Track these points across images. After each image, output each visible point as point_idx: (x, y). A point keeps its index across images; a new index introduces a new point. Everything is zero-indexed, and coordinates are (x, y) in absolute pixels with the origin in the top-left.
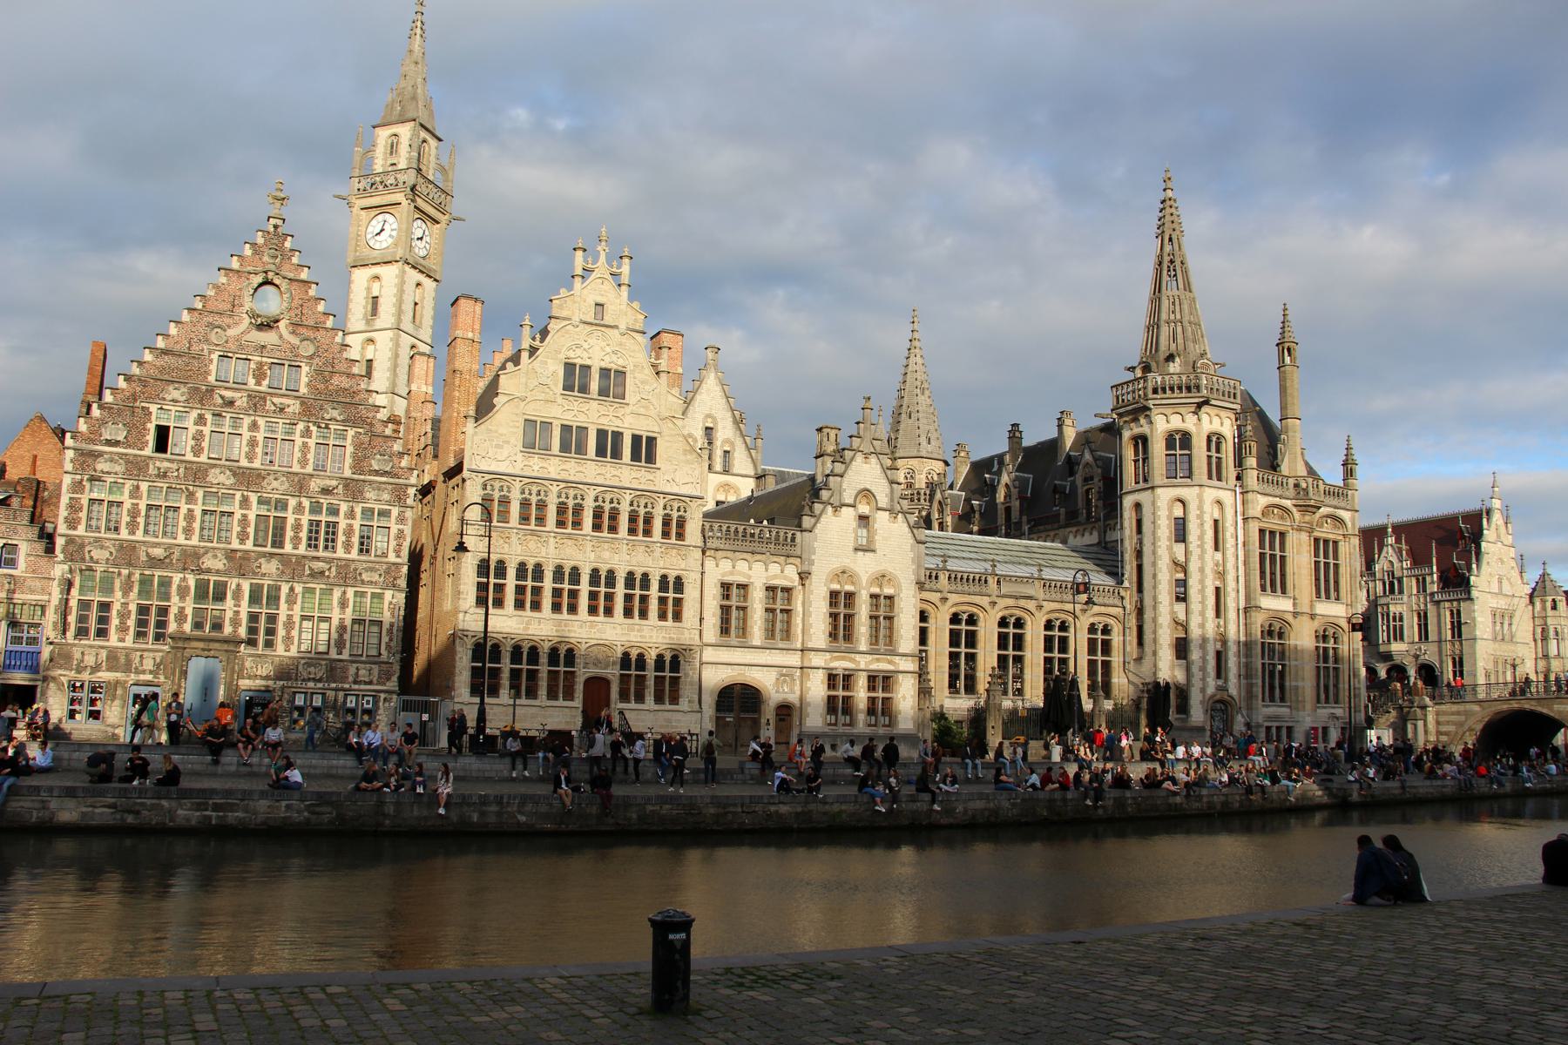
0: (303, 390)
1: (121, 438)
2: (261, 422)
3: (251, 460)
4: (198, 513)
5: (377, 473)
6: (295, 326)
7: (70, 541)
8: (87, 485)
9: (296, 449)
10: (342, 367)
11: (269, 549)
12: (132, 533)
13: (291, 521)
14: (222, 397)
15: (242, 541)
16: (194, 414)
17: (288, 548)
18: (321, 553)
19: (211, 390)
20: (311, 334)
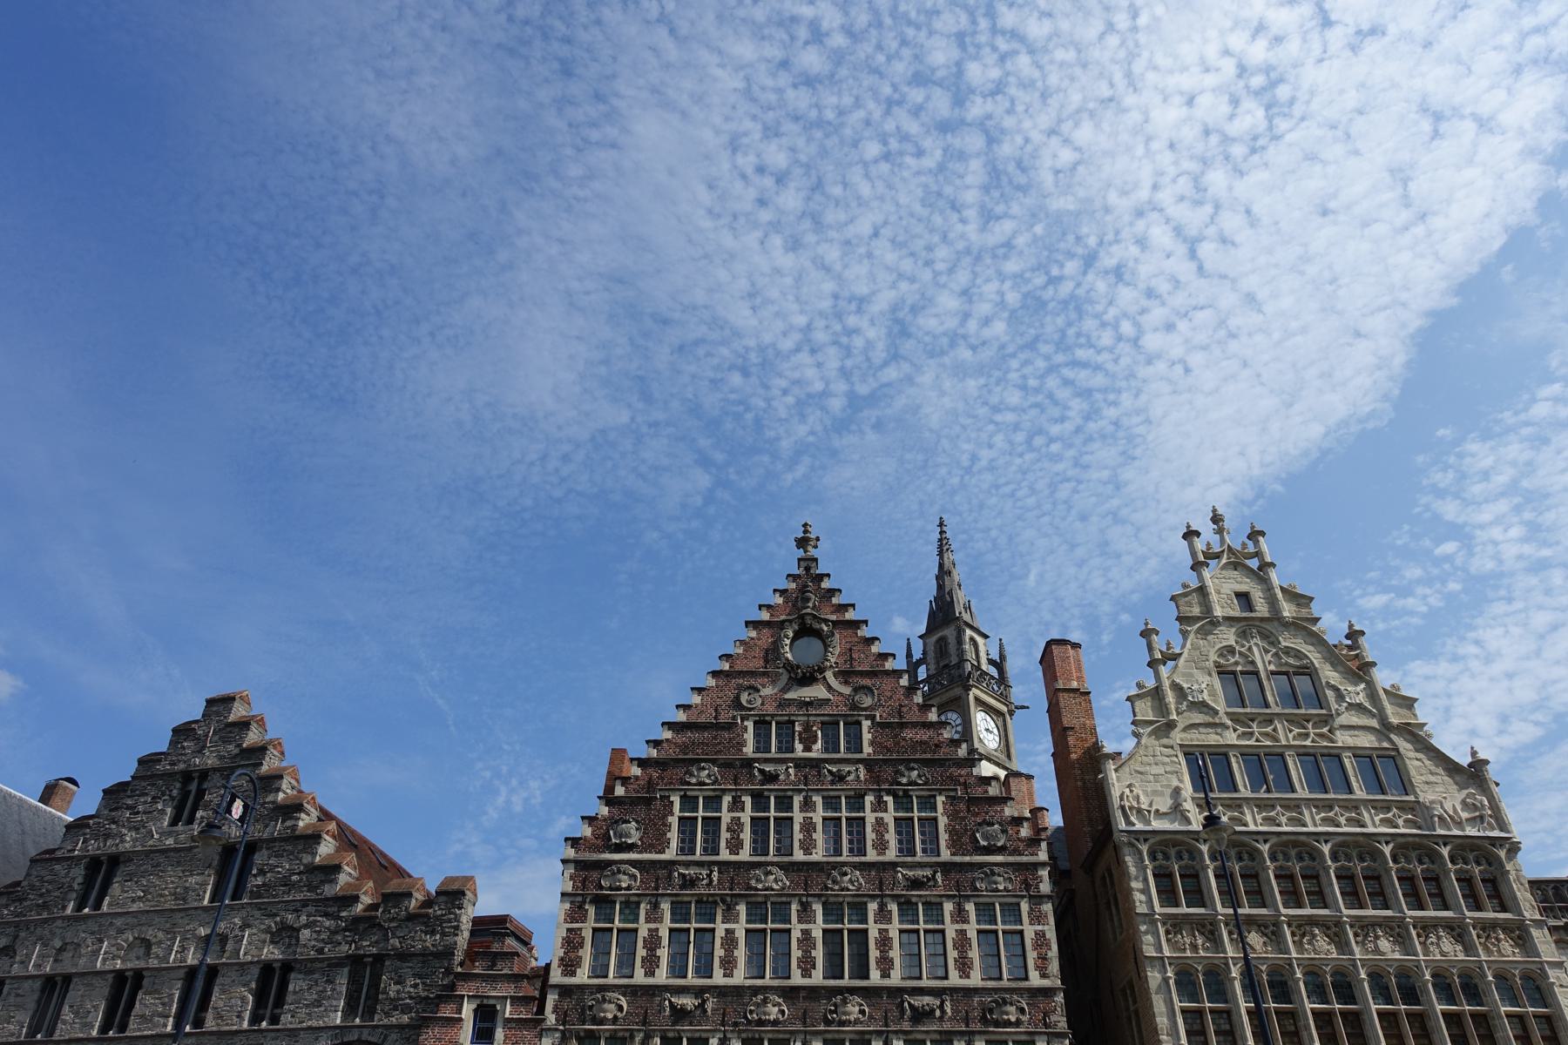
0: (867, 749)
1: (634, 838)
2: (818, 799)
3: (807, 850)
4: (741, 934)
5: (989, 850)
6: (845, 675)
7: (565, 991)
8: (591, 910)
9: (869, 829)
10: (913, 716)
11: (846, 982)
12: (650, 973)
13: (873, 934)
14: (762, 771)
15: (806, 973)
16: (727, 799)
17: (875, 977)
18: (925, 983)
19: (748, 763)
20: (867, 682)
